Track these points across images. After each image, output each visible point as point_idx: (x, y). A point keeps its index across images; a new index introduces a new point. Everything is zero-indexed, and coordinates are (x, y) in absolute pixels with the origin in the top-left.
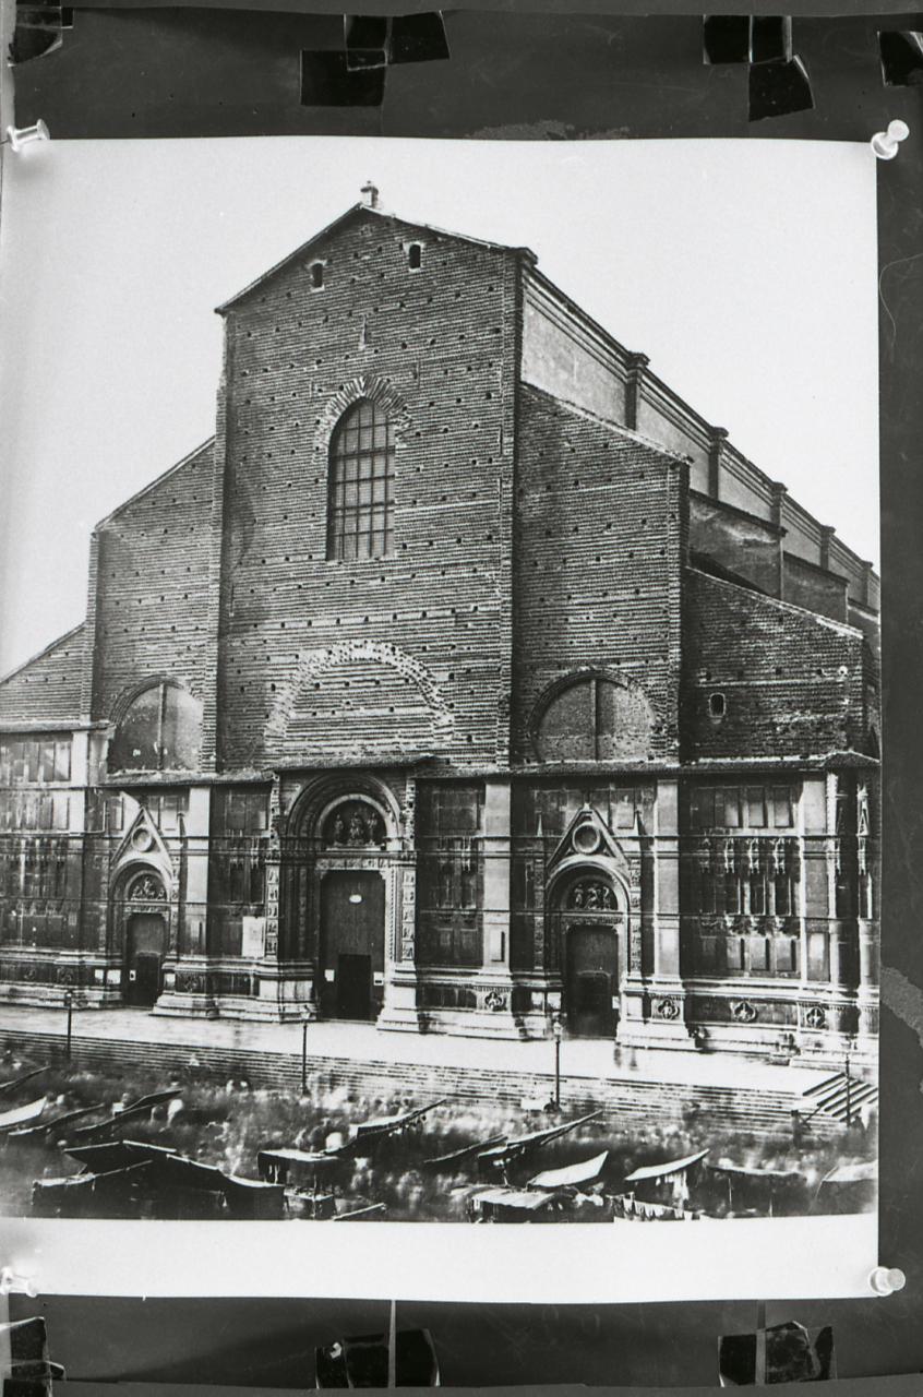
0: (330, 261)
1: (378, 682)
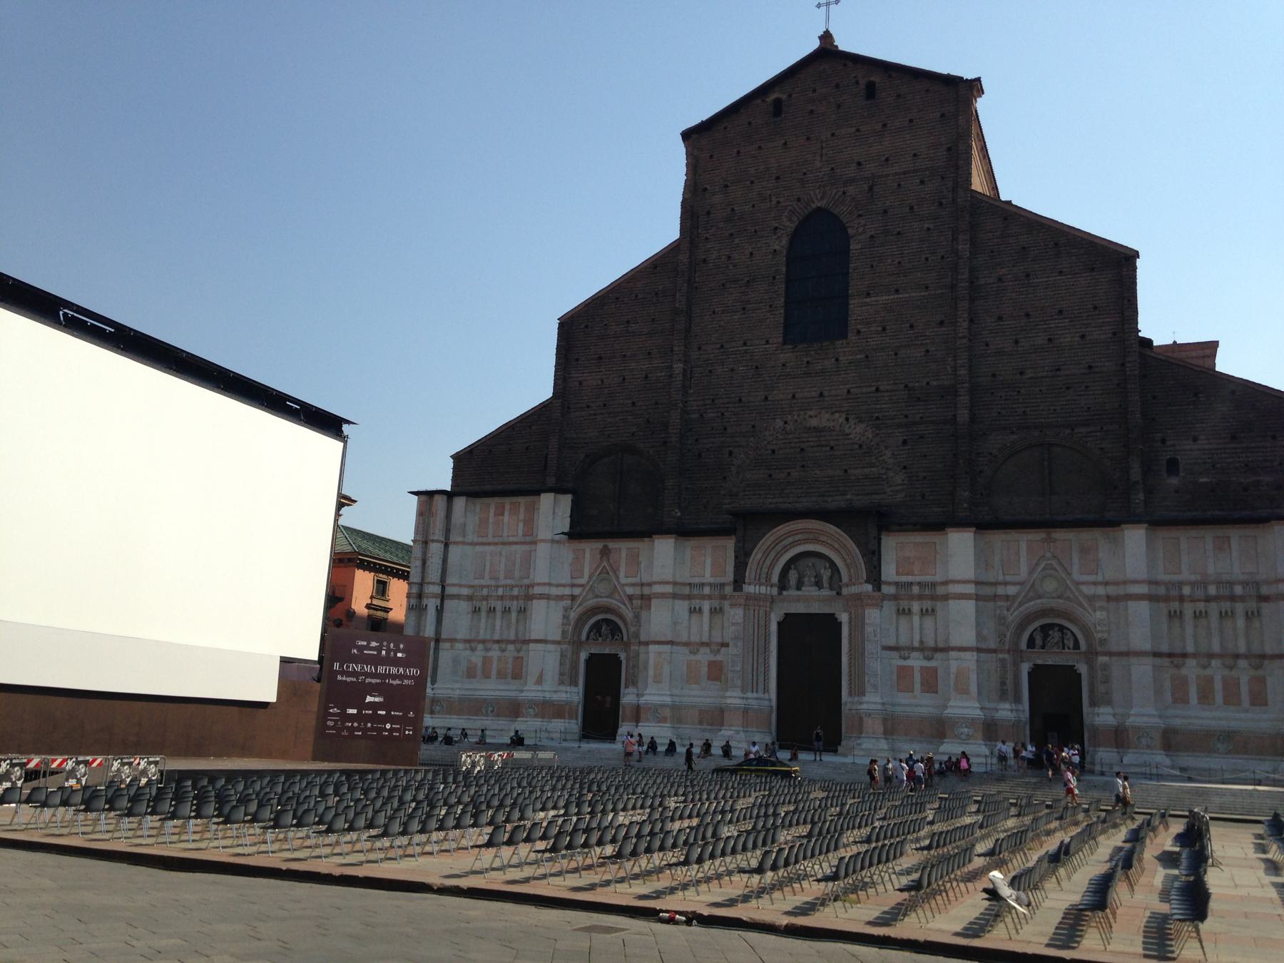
0: (790, 96)
1: (832, 448)
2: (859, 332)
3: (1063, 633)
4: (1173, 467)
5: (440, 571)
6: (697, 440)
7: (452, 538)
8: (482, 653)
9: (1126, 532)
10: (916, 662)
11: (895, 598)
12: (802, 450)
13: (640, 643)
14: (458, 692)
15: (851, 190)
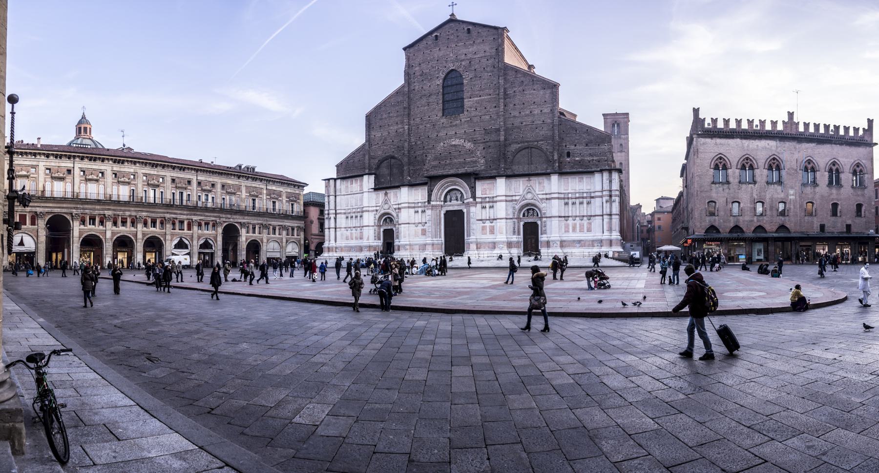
9: (552, 177)
10: (488, 224)
11: (481, 203)
13: (399, 224)
15: (463, 63)
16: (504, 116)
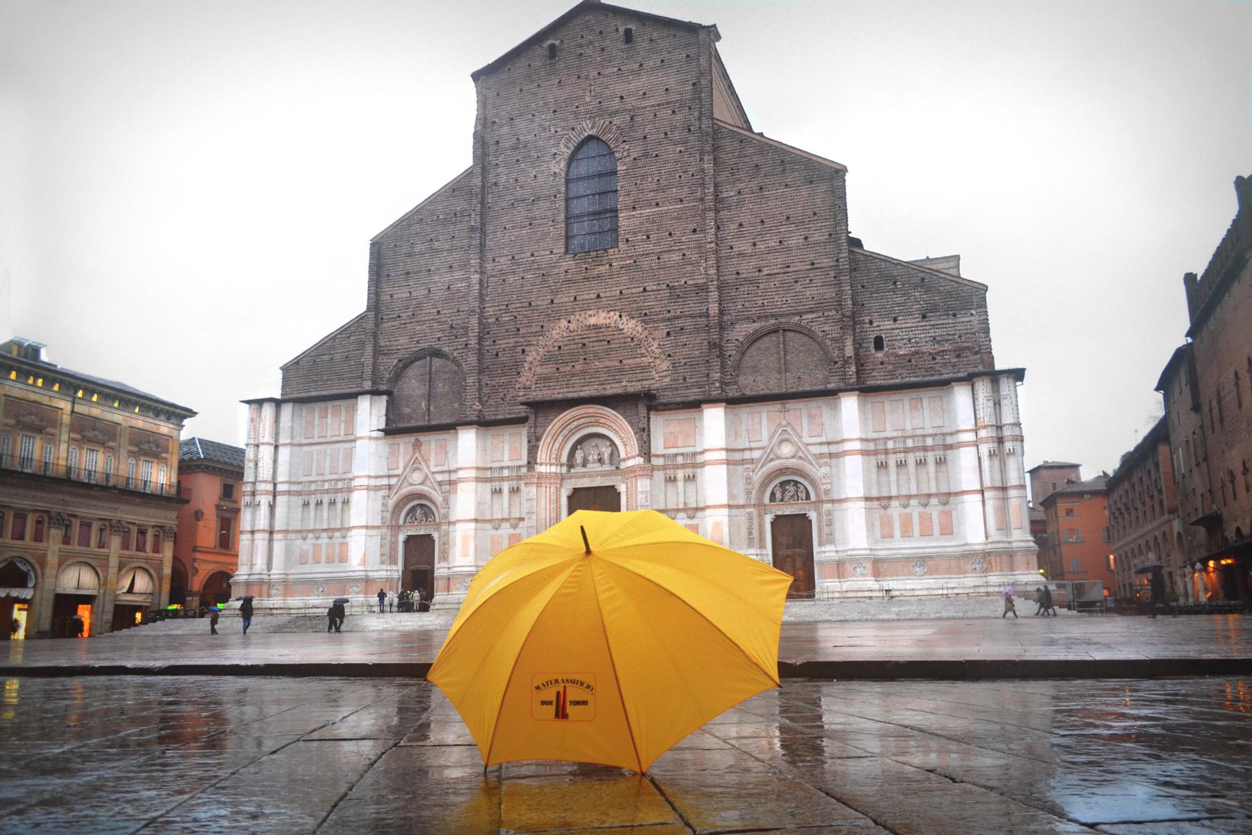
0: (562, 41)
1: (609, 342)
2: (627, 241)
3: (797, 487)
4: (879, 344)
5: (271, 470)
6: (494, 341)
7: (281, 441)
8: (313, 541)
11: (664, 468)
12: (584, 345)
13: (450, 523)
14: (292, 576)
16: (716, 252)
